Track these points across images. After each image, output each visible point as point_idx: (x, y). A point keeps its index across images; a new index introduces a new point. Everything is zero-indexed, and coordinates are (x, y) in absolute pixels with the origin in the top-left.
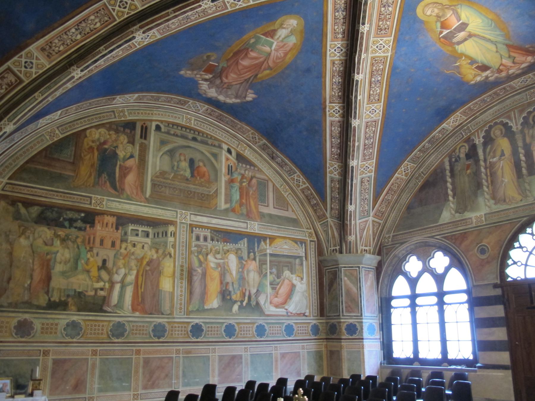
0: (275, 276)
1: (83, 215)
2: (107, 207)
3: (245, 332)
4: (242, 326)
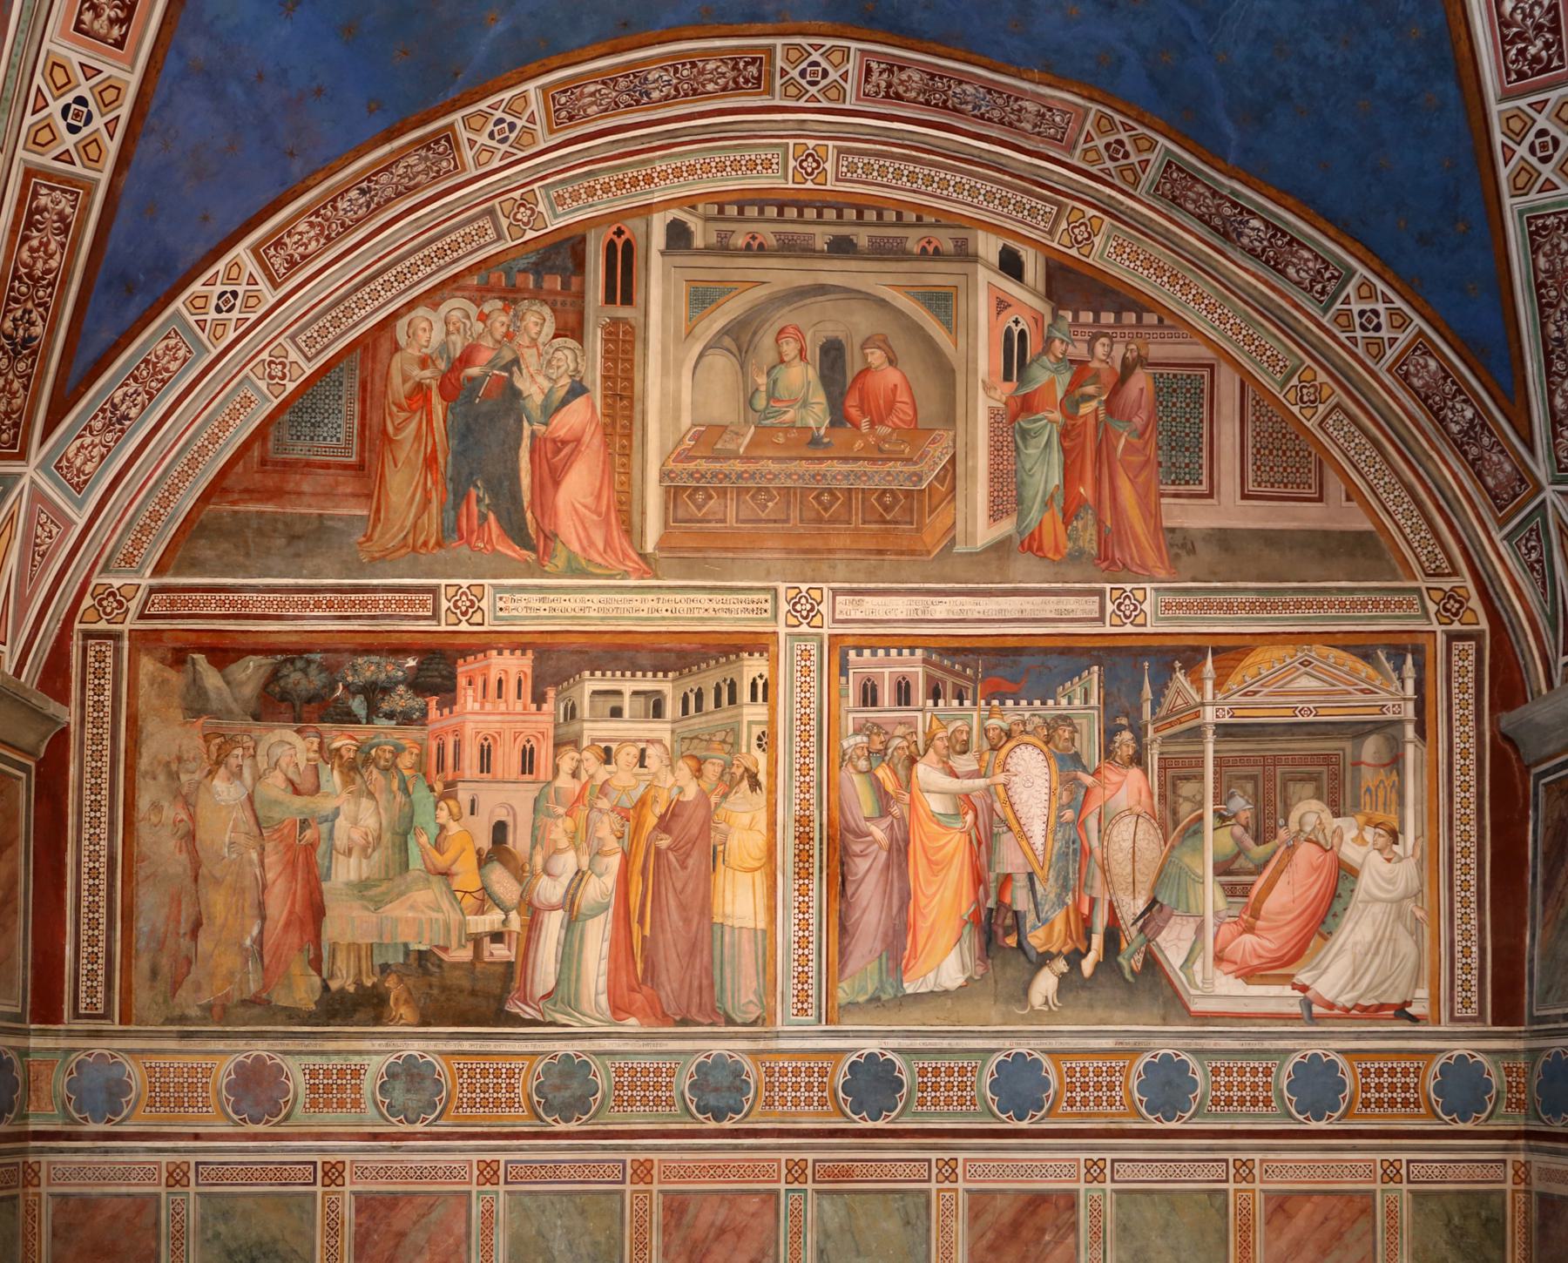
0: (1246, 828)
1: (411, 662)
2: (496, 618)
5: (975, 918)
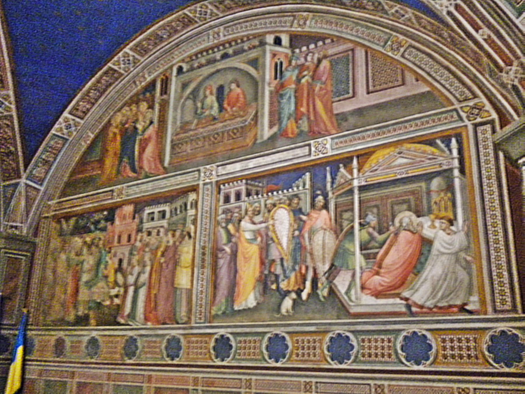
0: (374, 228)
3: (306, 351)
4: (300, 338)
5: (259, 280)
